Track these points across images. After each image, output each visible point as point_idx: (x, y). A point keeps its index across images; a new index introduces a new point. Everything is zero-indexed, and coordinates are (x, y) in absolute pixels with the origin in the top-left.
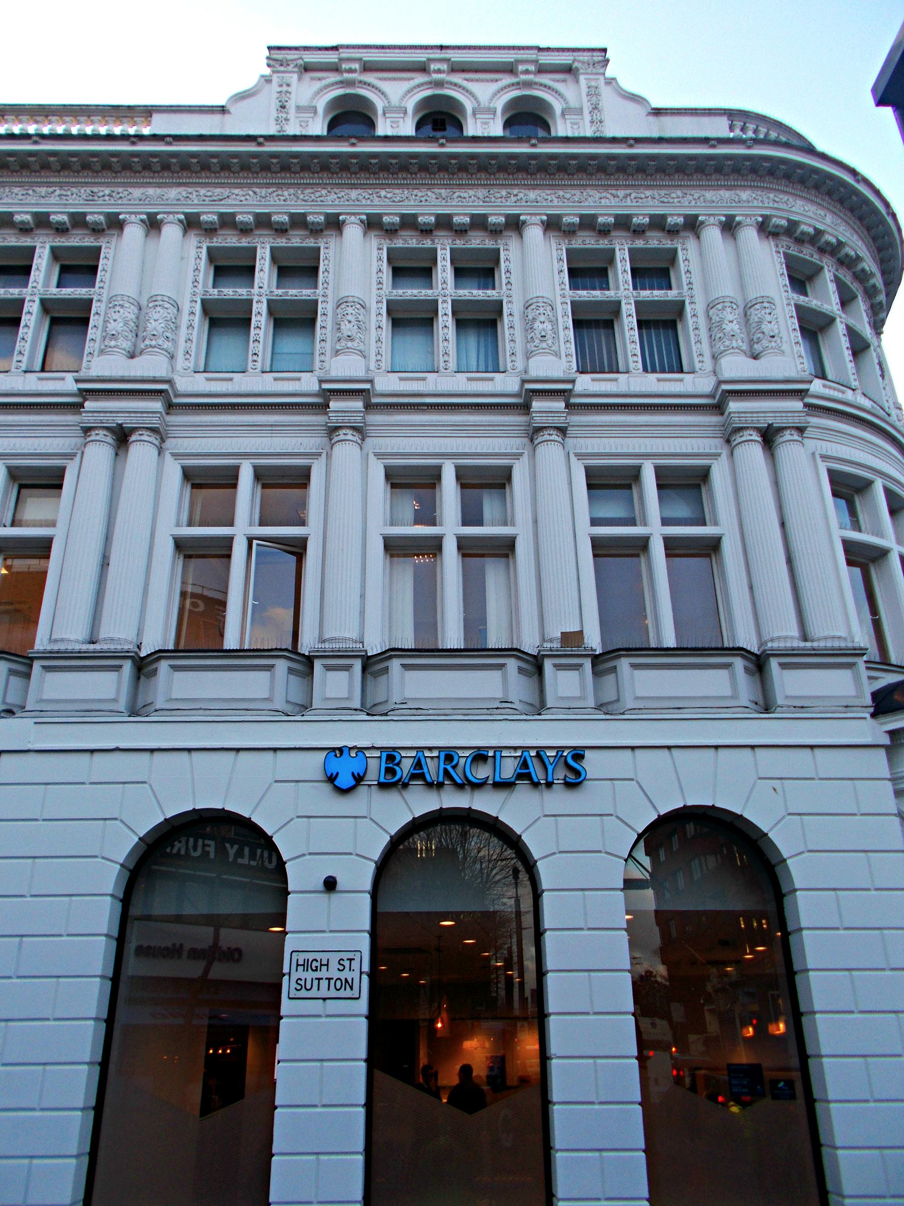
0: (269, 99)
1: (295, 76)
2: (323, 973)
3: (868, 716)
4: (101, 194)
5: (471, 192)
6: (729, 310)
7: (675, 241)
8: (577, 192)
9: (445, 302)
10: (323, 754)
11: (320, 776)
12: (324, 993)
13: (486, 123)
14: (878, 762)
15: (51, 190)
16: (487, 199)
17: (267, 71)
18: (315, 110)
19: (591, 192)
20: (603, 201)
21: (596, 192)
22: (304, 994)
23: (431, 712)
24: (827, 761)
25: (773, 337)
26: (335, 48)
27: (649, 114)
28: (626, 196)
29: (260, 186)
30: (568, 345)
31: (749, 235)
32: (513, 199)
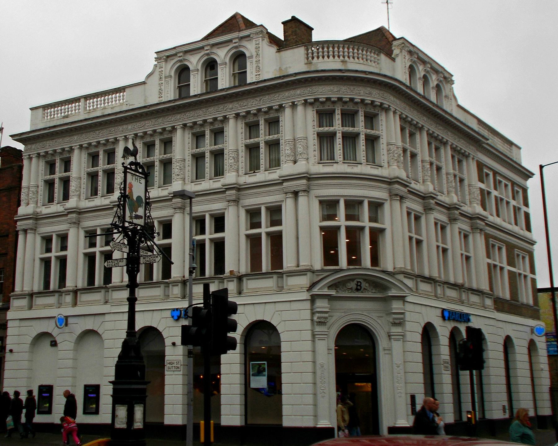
0: (156, 76)
1: (164, 63)
2: (173, 365)
3: (306, 291)
4: (112, 131)
5: (213, 108)
6: (288, 145)
7: (279, 113)
8: (244, 101)
9: (207, 152)
10: (170, 311)
11: (171, 316)
12: (174, 370)
13: (222, 70)
14: (308, 305)
15: (100, 131)
16: (217, 111)
17: (156, 63)
18: (171, 76)
19: (249, 100)
20: (254, 103)
21: (250, 100)
22: (169, 370)
23: (196, 297)
24: (295, 306)
25: (300, 154)
26: (174, 48)
27: (277, 52)
28: (260, 100)
29: (153, 119)
30: (242, 164)
31: (300, 109)
32: (225, 109)
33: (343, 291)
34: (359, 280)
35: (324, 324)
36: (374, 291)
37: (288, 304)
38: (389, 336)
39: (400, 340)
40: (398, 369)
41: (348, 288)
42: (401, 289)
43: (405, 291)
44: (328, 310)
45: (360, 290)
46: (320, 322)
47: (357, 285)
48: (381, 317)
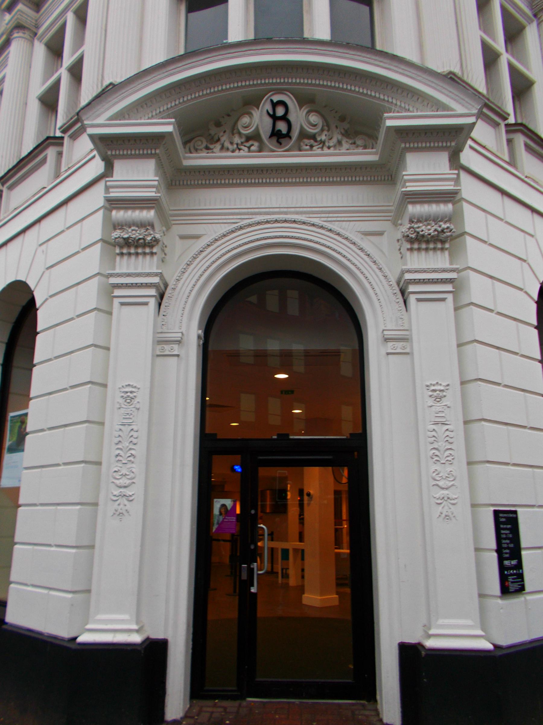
33: (233, 151)
34: (276, 98)
35: (147, 250)
36: (345, 145)
37: (61, 212)
38: (403, 292)
39: (443, 300)
40: (438, 407)
41: (249, 138)
42: (439, 105)
43: (453, 110)
44: (151, 193)
45: (288, 135)
46: (127, 243)
47: (274, 118)
48: (380, 234)
